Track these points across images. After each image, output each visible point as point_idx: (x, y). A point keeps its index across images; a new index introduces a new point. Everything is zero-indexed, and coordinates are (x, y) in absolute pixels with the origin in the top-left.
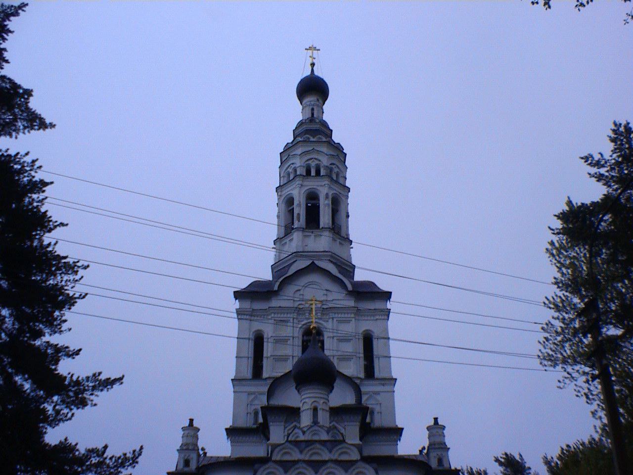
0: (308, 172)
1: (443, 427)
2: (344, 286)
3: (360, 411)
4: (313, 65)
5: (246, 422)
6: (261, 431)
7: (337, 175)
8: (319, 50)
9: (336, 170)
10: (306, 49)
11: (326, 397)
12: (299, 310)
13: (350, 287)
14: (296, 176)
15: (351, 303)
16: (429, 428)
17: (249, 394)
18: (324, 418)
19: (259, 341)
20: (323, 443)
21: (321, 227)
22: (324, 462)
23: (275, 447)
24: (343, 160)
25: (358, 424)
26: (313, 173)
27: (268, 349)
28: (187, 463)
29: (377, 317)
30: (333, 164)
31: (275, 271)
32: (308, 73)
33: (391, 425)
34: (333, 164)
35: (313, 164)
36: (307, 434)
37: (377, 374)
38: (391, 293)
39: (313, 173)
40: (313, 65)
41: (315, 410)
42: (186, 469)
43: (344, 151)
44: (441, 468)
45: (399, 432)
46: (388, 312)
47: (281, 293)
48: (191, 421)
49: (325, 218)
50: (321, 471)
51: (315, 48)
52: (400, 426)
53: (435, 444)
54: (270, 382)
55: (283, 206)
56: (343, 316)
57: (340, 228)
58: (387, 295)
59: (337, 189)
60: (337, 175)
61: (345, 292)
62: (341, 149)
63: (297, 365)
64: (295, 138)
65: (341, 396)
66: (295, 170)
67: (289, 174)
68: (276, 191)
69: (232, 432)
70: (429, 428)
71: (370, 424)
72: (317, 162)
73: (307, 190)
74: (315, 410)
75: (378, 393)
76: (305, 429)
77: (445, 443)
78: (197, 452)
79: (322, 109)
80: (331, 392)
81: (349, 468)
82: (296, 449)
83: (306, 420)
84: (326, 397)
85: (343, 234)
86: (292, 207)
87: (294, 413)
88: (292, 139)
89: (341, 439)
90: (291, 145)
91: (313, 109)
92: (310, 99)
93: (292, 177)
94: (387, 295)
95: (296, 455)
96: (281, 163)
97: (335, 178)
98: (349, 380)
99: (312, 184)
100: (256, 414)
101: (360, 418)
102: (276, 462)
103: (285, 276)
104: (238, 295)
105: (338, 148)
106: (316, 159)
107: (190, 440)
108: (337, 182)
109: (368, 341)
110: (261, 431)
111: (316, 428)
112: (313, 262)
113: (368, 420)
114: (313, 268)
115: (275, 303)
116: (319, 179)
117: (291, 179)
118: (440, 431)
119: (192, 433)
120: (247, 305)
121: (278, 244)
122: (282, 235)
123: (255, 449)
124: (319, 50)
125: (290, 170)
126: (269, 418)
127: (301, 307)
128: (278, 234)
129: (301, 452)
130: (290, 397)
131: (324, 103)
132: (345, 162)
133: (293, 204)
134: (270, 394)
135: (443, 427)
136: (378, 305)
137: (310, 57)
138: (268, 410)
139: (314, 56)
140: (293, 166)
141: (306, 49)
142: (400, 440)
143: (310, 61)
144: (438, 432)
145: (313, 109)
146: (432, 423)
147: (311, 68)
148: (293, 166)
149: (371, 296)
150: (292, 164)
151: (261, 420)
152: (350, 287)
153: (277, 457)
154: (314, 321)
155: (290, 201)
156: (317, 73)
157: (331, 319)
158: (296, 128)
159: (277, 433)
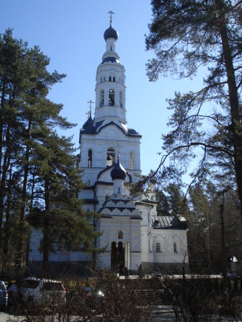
0: (110, 79)
4: (111, 22)
7: (122, 81)
9: (121, 78)
15: (126, 138)
20: (123, 201)
22: (124, 208)
26: (112, 79)
39: (112, 79)
40: (111, 22)
47: (99, 134)
58: (141, 136)
60: (122, 81)
66: (105, 78)
67: (101, 79)
94: (141, 137)
114: (112, 123)
115: (97, 137)
116: (114, 83)
125: (102, 77)
136: (136, 139)
138: (98, 183)
148: (104, 75)
149: (132, 134)
154: (113, 146)
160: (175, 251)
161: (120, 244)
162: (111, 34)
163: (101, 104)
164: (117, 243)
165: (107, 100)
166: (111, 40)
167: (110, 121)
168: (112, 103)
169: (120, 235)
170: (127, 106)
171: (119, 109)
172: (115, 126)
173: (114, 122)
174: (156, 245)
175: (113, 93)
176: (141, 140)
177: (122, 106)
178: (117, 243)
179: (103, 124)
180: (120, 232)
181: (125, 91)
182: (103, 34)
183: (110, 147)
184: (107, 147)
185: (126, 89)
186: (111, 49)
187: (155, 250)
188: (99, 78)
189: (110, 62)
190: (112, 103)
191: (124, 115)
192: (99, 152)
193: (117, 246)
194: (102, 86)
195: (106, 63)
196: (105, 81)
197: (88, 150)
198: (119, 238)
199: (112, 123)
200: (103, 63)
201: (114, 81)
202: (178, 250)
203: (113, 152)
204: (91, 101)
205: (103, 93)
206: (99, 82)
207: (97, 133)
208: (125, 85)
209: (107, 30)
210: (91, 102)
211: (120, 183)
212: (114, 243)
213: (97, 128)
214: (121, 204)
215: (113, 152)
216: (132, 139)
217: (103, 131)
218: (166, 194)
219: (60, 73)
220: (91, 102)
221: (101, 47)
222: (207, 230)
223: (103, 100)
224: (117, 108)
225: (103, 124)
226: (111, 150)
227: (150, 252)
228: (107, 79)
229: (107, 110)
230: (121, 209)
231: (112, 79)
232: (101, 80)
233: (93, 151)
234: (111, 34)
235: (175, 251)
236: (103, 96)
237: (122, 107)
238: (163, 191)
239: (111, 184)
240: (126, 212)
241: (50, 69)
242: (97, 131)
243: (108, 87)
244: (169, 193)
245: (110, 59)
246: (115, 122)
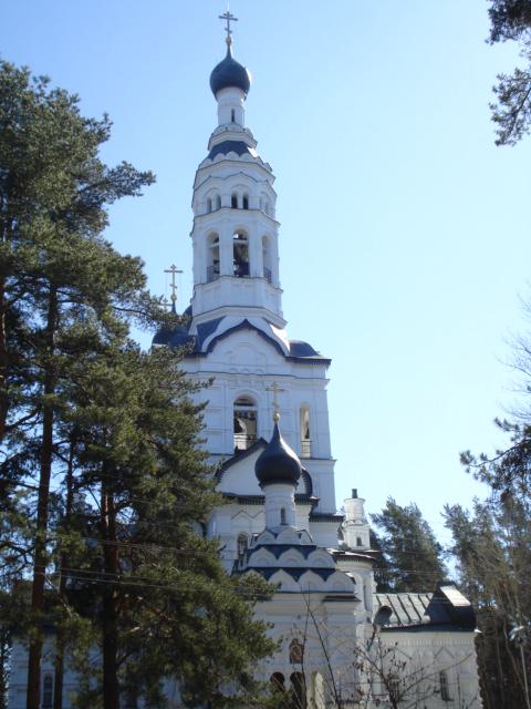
0: (234, 204)
2: (283, 354)
4: (229, 42)
7: (267, 207)
9: (265, 200)
15: (288, 368)
20: (297, 547)
26: (240, 203)
32: (222, 57)
39: (240, 203)
40: (229, 42)
44: (360, 548)
47: (211, 356)
60: (267, 207)
61: (281, 358)
67: (210, 202)
92: (230, 94)
94: (327, 362)
114: (246, 325)
125: (213, 196)
140: (216, 192)
148: (216, 192)
149: (302, 355)
162: (229, 78)
163: (214, 272)
164: (287, 677)
165: (227, 264)
167: (239, 320)
168: (243, 269)
170: (286, 275)
171: (262, 285)
172: (255, 333)
173: (252, 321)
175: (244, 242)
176: (330, 373)
177: (269, 276)
178: (287, 677)
179: (221, 329)
181: (276, 235)
182: (209, 79)
183: (245, 393)
185: (280, 230)
186: (233, 120)
188: (200, 198)
189: (232, 155)
190: (243, 269)
191: (277, 303)
195: (220, 156)
198: (293, 660)
199: (246, 325)
200: (211, 156)
201: (246, 206)
203: (253, 409)
204: (173, 267)
205: (217, 240)
206: (203, 209)
207: (204, 355)
208: (276, 219)
209: (218, 67)
210: (173, 270)
211: (285, 494)
214: (292, 558)
215: (253, 409)
216: (303, 371)
217: (221, 347)
219: (141, 168)
220: (173, 270)
222: (517, 634)
223: (216, 262)
224: (258, 282)
225: (221, 329)
226: (244, 401)
228: (227, 201)
229: (230, 289)
230: (296, 572)
231: (240, 203)
234: (229, 78)
236: (216, 250)
237: (270, 281)
239: (259, 500)
240: (309, 579)
241: (109, 156)
243: (227, 226)
244: (390, 529)
245: (230, 145)
246: (255, 321)
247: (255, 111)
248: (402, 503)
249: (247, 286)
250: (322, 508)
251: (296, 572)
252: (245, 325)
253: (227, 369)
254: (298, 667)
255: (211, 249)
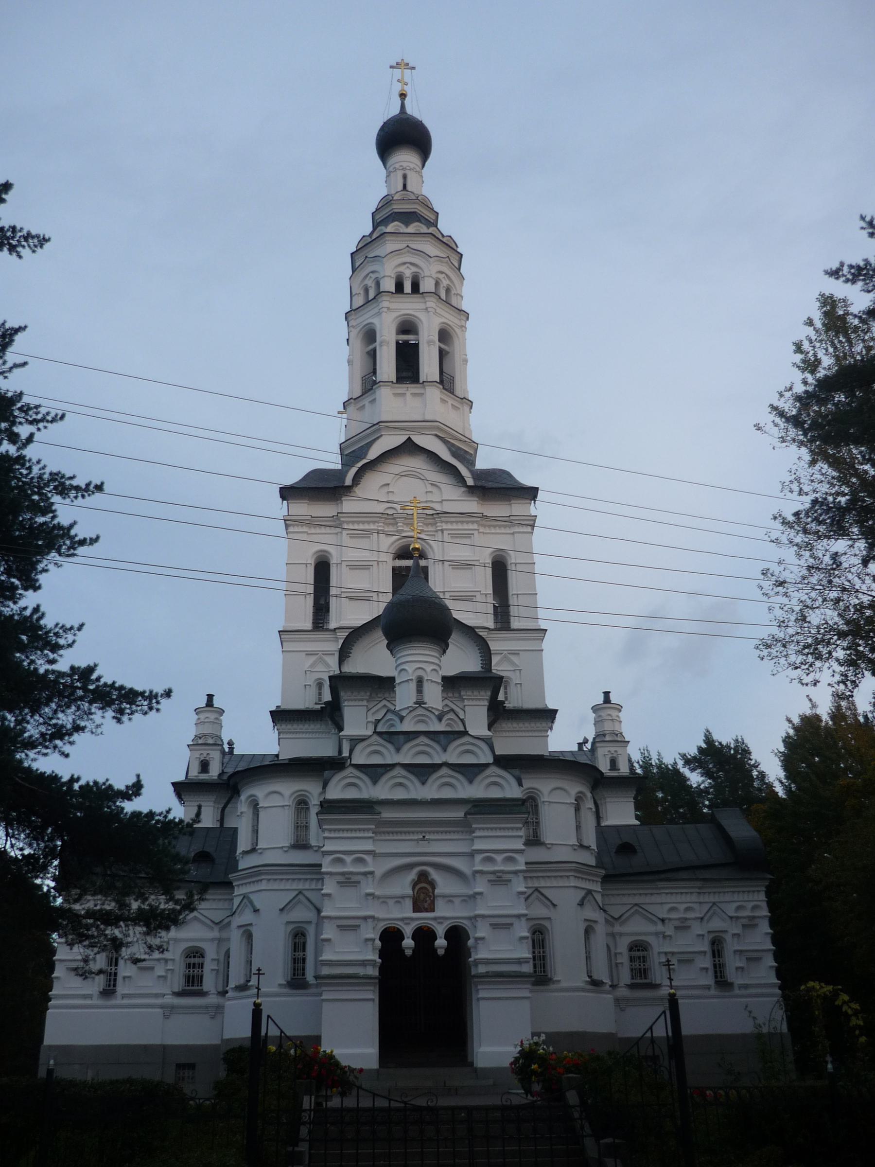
0: (399, 287)
1: (619, 708)
2: (461, 480)
3: (488, 681)
4: (403, 96)
5: (305, 701)
6: (330, 714)
7: (448, 290)
8: (413, 68)
9: (445, 282)
10: (391, 67)
11: (437, 661)
12: (389, 518)
13: (470, 482)
14: (379, 293)
15: (472, 505)
16: (595, 709)
17: (309, 654)
18: (434, 696)
19: (322, 569)
20: (432, 735)
21: (421, 381)
23: (355, 741)
24: (457, 265)
25: (486, 703)
26: (408, 288)
27: (339, 579)
28: (204, 766)
29: (517, 529)
30: (442, 273)
31: (346, 453)
32: (395, 111)
33: (540, 706)
34: (442, 273)
35: (408, 273)
36: (406, 721)
37: (515, 624)
38: (537, 489)
39: (408, 288)
40: (403, 96)
41: (420, 682)
42: (204, 777)
43: (459, 250)
45: (550, 715)
46: (531, 522)
48: (210, 697)
49: (429, 366)
50: (430, 781)
51: (407, 64)
52: (551, 706)
53: (604, 735)
54: (344, 634)
55: (358, 343)
56: (460, 526)
57: (452, 380)
59: (448, 318)
60: (448, 290)
62: (455, 247)
63: (391, 608)
64: (375, 226)
65: (460, 659)
66: (378, 284)
67: (367, 291)
68: (346, 318)
69: (279, 716)
70: (595, 709)
71: (503, 702)
72: (414, 269)
73: (397, 317)
74: (420, 682)
75: (516, 653)
76: (404, 713)
77: (621, 733)
78: (220, 748)
79: (422, 176)
80: (444, 652)
81: (476, 775)
82: (389, 745)
83: (404, 697)
84: (437, 661)
85: (458, 392)
86: (371, 347)
87: (382, 685)
88: (371, 229)
89: (462, 729)
90: (370, 240)
91: (405, 177)
93: (372, 295)
94: (531, 493)
95: (390, 756)
96: (353, 271)
97: (443, 295)
98: (470, 632)
99: (408, 306)
100: (320, 685)
101: (489, 693)
102: (358, 767)
103: (360, 460)
104: (287, 493)
105: (449, 245)
106: (411, 264)
107: (207, 729)
108: (447, 302)
109: (500, 569)
110: (330, 714)
111: (420, 711)
112: (409, 438)
113: (501, 697)
114: (409, 448)
115: (349, 505)
116: (416, 298)
117: (370, 298)
118: (614, 713)
119: (212, 716)
120: (302, 508)
121: (351, 409)
122: (358, 393)
123: (314, 744)
124: (413, 68)
125: (370, 283)
126: (342, 694)
127: (390, 512)
128: (351, 391)
129: (398, 750)
130: (374, 659)
131: (423, 166)
132: (459, 269)
133: (375, 341)
134: (344, 654)
135: (619, 708)
136: (517, 508)
137: (398, 81)
138: (339, 682)
139: (406, 79)
140: (374, 276)
141: (391, 67)
142: (551, 728)
143: (397, 88)
144: (610, 715)
145: (405, 177)
146: (600, 700)
147: (400, 102)
150: (373, 272)
151: (327, 696)
152: (470, 482)
153: (359, 758)
155: (370, 336)
156: (412, 110)
157: (440, 532)
158: (377, 210)
159: (357, 719)
160: (722, 983)
161: (424, 935)
162: (403, 136)
163: (369, 384)
164: (408, 931)
165: (387, 366)
166: (405, 158)
169: (423, 896)
170: (475, 379)
171: (434, 394)
173: (419, 440)
174: (624, 959)
177: (446, 382)
178: (408, 931)
180: (423, 877)
181: (463, 328)
184: (388, 544)
186: (405, 186)
187: (625, 977)
192: (355, 567)
193: (408, 943)
194: (366, 317)
195: (382, 229)
196: (379, 293)
197: (312, 561)
198: (416, 909)
202: (731, 975)
207: (349, 489)
212: (390, 937)
213: (347, 472)
218: (695, 778)
221: (370, 182)
225: (374, 453)
227: (596, 983)
228: (389, 285)
229: (394, 404)
232: (366, 299)
233: (333, 561)
234: (403, 136)
235: (722, 983)
238: (686, 771)
242: (348, 481)
244: (707, 774)
245: (403, 216)
247: (437, 181)
248: (724, 737)
249: (414, 395)
250: (514, 699)
251: (423, 772)
252: (409, 448)
253: (381, 508)
254: (424, 916)
255: (368, 353)
